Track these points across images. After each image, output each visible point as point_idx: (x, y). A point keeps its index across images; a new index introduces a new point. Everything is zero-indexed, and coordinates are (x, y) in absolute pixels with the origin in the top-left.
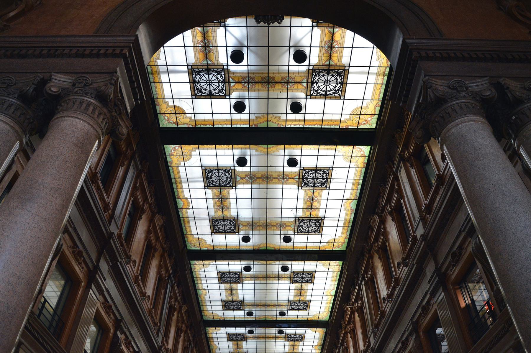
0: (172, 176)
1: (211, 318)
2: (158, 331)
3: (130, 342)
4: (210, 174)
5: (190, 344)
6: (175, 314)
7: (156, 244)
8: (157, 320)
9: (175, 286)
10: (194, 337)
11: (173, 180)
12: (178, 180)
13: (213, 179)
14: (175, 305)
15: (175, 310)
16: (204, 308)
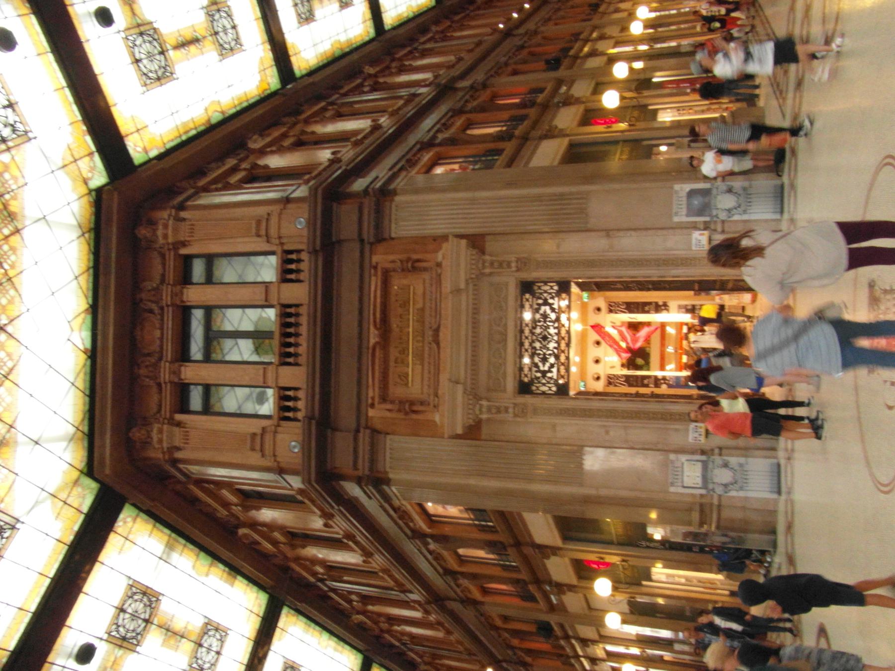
0: (178, 141)
1: (370, 25)
2: (415, 95)
3: (444, 124)
4: (150, 75)
5: (416, 49)
6: (381, 80)
7: (294, 136)
8: (401, 102)
9: (342, 91)
10: (403, 46)
11: (184, 138)
12: (182, 131)
13: (157, 67)
14: (369, 85)
15: (376, 83)
16: (359, 41)
